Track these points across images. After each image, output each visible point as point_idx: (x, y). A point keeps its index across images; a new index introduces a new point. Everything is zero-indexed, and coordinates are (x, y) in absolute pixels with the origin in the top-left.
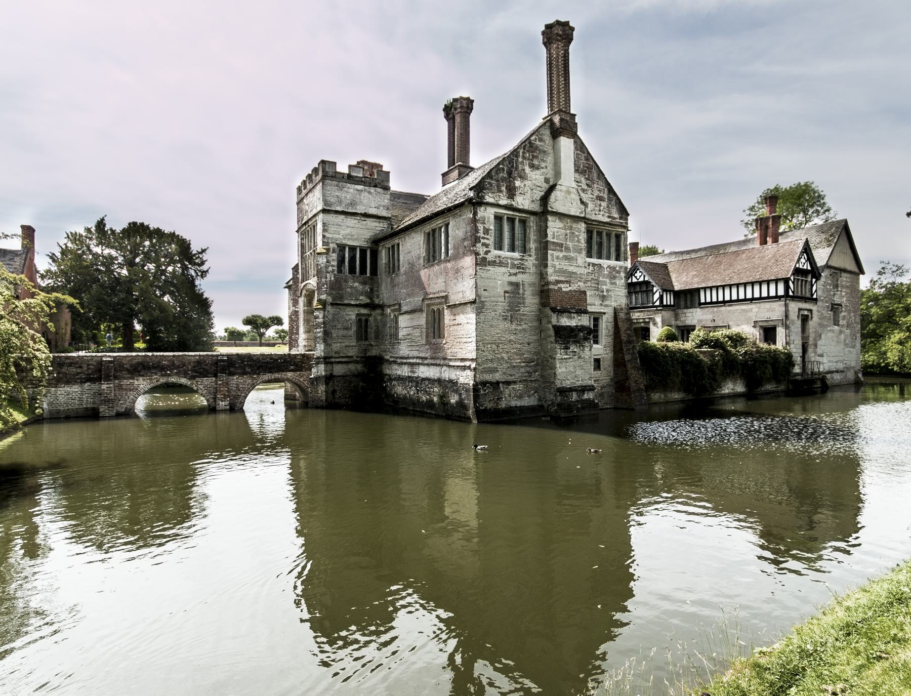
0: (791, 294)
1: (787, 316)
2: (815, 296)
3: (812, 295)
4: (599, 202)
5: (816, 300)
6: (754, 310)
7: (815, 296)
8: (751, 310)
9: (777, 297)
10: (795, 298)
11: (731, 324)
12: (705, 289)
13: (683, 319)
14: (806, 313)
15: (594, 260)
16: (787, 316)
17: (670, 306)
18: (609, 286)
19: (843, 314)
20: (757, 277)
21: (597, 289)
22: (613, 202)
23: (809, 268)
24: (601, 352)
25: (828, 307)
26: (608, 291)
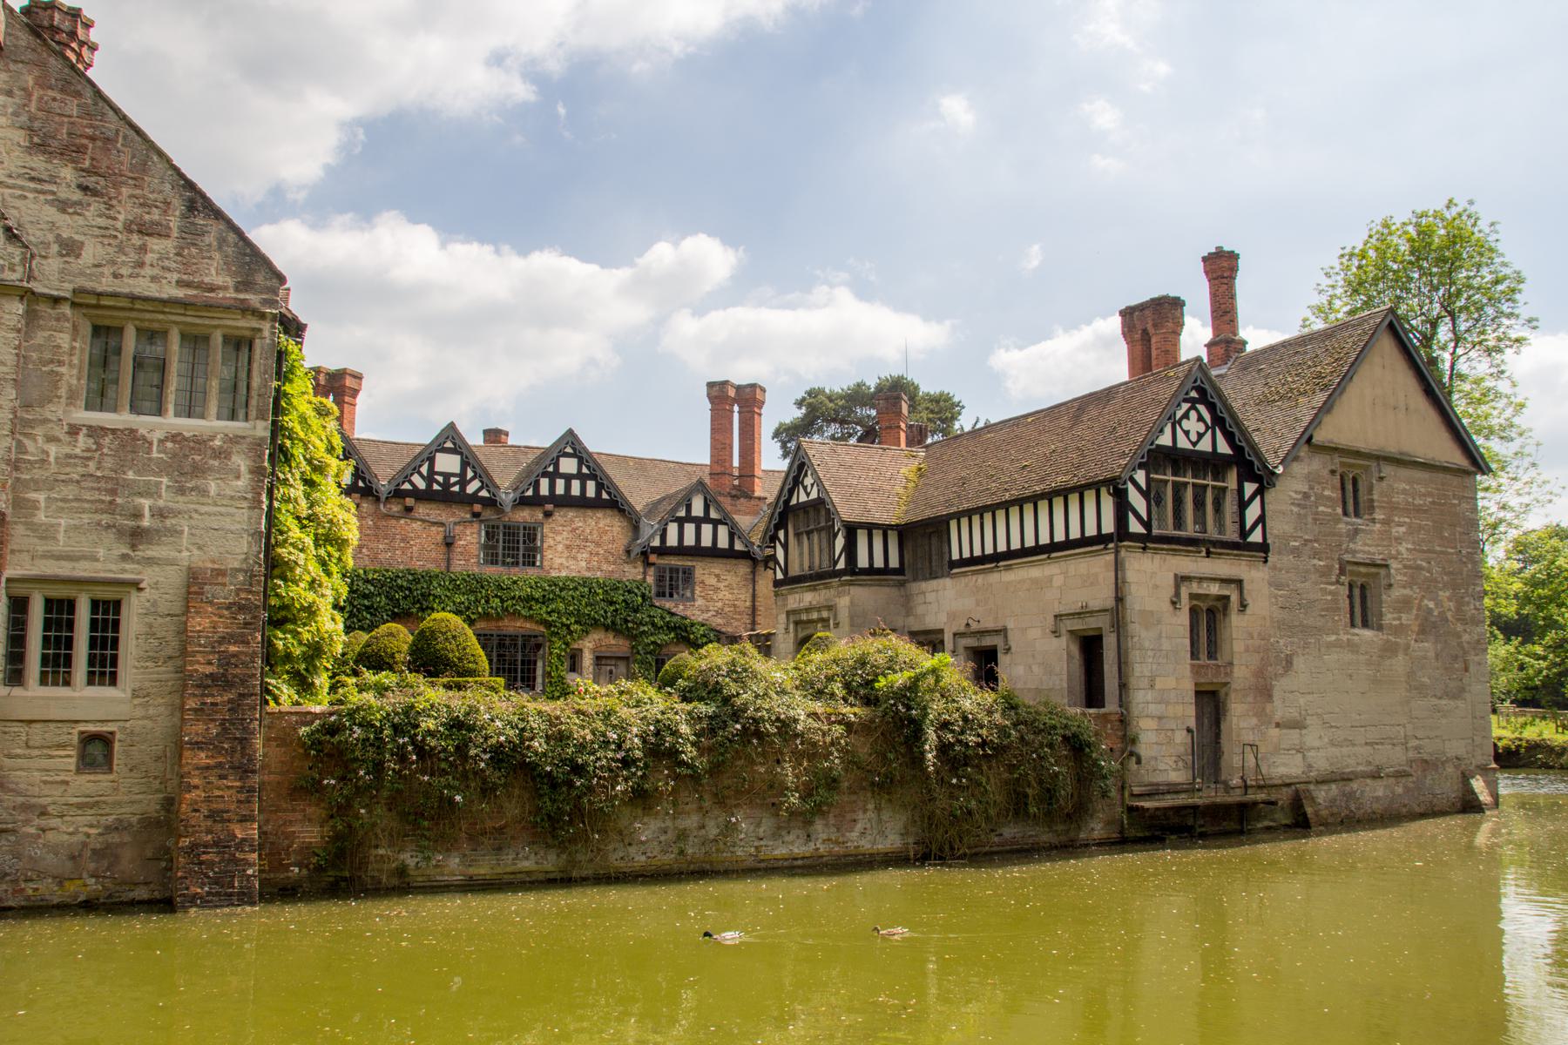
0: (1135, 527)
1: (1119, 599)
2: (1256, 537)
3: (1244, 533)
4: (136, 239)
5: (1263, 548)
6: (1058, 581)
7: (1256, 537)
8: (1050, 579)
9: (1101, 539)
10: (1147, 541)
11: (1010, 625)
12: (958, 516)
13: (920, 610)
14: (1215, 589)
15: (121, 419)
16: (1119, 599)
17: (886, 571)
18: (166, 499)
19: (1397, 593)
20: (1081, 477)
21: (111, 508)
22: (211, 239)
23: (1224, 448)
24: (123, 710)
25: (1324, 573)
26: (160, 514)
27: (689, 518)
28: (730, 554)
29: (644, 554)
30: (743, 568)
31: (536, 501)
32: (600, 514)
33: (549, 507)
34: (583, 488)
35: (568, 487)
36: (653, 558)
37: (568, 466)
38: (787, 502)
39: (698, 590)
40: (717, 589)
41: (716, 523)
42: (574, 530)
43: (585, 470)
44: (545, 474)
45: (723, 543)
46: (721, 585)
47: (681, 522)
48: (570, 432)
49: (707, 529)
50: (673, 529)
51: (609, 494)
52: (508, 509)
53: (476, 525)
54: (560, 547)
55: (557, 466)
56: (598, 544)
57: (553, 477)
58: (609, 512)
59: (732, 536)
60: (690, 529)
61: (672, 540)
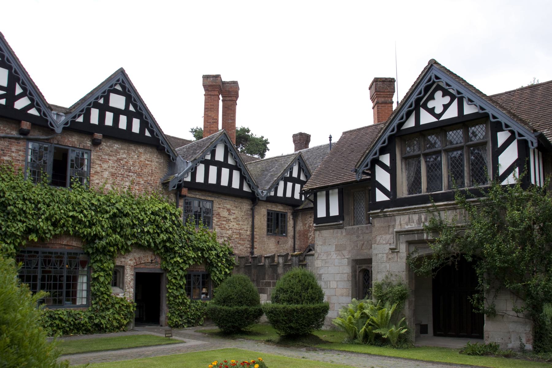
27: (213, 162)
28: (237, 195)
29: (179, 187)
30: (246, 206)
31: (86, 129)
32: (141, 150)
33: (98, 136)
34: (130, 124)
35: (116, 120)
36: (185, 191)
37: (117, 101)
38: (401, 125)
39: (215, 220)
40: (228, 221)
41: (231, 168)
42: (119, 160)
43: (131, 108)
44: (96, 105)
45: (236, 185)
46: (231, 217)
47: (207, 164)
48: (122, 72)
49: (225, 172)
50: (201, 169)
51: (151, 132)
52: (59, 130)
53: (22, 143)
54: (106, 174)
55: (107, 100)
56: (139, 175)
57: (104, 108)
58: (149, 149)
59: (242, 178)
60: (213, 170)
61: (200, 179)
